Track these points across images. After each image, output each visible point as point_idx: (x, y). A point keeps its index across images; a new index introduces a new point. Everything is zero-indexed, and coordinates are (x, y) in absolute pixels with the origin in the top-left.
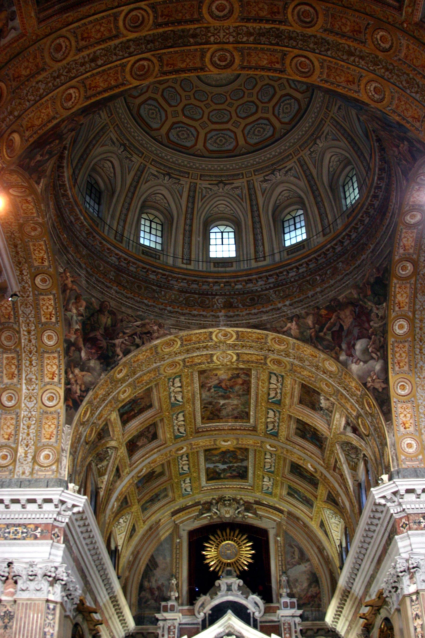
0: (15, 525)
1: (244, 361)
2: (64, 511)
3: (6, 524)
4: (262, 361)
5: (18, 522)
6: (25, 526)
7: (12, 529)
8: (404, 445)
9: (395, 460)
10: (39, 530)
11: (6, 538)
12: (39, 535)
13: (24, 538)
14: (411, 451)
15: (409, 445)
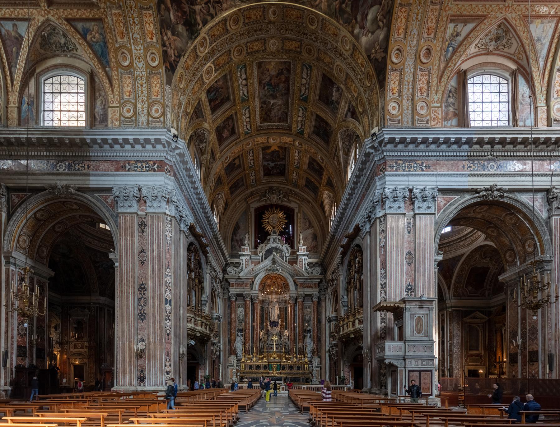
0: (140, 162)
1: (286, 50)
2: (171, 151)
3: (134, 161)
4: (299, 50)
5: (142, 159)
6: (147, 162)
7: (139, 165)
8: (390, 108)
9: (383, 120)
10: (156, 165)
11: (136, 171)
12: (156, 169)
13: (147, 171)
14: (394, 112)
15: (394, 108)
